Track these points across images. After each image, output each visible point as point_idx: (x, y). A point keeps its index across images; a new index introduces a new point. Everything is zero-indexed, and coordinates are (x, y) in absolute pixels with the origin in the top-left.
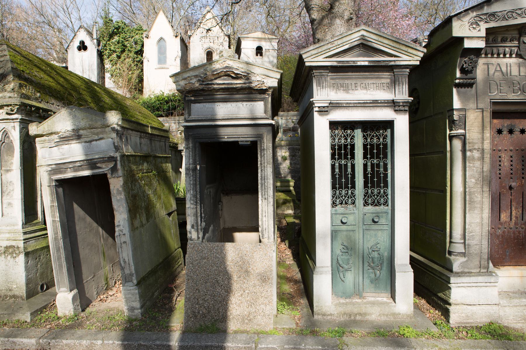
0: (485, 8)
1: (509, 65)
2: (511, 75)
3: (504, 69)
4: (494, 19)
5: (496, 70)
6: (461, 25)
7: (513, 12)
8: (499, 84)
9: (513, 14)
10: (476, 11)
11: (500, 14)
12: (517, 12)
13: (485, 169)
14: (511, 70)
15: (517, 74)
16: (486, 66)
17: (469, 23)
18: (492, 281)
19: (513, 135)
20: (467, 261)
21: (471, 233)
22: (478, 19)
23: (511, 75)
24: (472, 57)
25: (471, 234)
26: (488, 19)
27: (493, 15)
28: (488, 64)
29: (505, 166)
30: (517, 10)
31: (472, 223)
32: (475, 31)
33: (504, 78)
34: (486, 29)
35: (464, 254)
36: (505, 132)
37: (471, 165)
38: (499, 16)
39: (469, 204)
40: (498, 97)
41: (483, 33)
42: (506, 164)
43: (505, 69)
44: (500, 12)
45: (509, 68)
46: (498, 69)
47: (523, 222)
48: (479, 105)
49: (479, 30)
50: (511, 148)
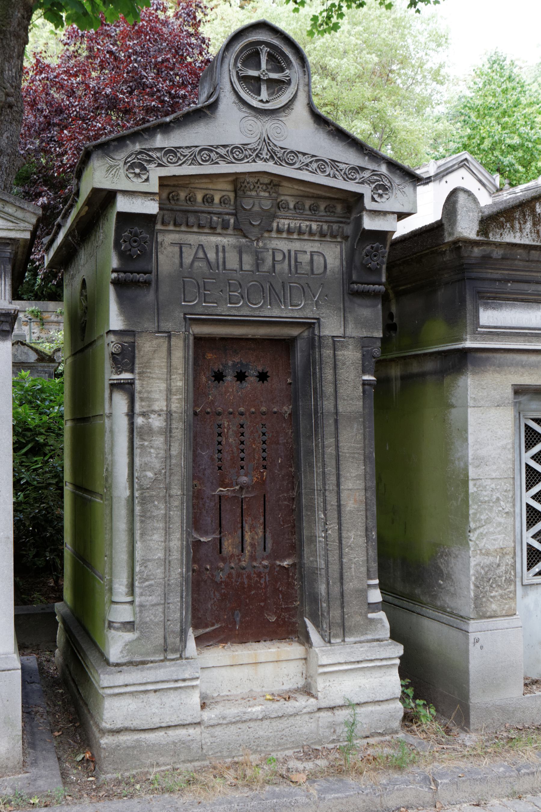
0: (159, 137)
1: (220, 249)
2: (224, 268)
3: (211, 256)
4: (175, 160)
5: (196, 258)
6: (111, 166)
7: (212, 151)
8: (201, 284)
9: (212, 155)
10: (140, 142)
11: (186, 152)
12: (218, 150)
13: (174, 451)
14: (224, 258)
15: (236, 266)
16: (177, 249)
17: (125, 163)
18: (187, 676)
19: (245, 384)
20: (138, 639)
21: (147, 580)
22: (145, 157)
23: (224, 268)
24: (137, 229)
25: (147, 583)
26: (165, 160)
27: (172, 151)
28: (181, 246)
29: (230, 446)
30: (217, 147)
31: (149, 560)
32: (140, 180)
33: (211, 274)
34: (160, 178)
35: (129, 626)
36: (229, 378)
37: (146, 443)
38: (185, 156)
39: (142, 522)
40: (200, 310)
41: (154, 186)
42: (231, 440)
43: (214, 255)
44: (187, 147)
45: (221, 255)
46: (201, 255)
47: (265, 554)
48: (162, 324)
49: (147, 180)
50: (242, 409)
